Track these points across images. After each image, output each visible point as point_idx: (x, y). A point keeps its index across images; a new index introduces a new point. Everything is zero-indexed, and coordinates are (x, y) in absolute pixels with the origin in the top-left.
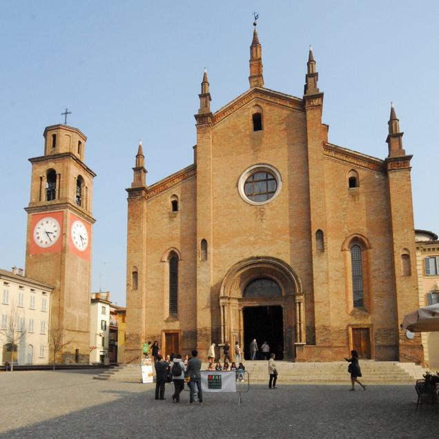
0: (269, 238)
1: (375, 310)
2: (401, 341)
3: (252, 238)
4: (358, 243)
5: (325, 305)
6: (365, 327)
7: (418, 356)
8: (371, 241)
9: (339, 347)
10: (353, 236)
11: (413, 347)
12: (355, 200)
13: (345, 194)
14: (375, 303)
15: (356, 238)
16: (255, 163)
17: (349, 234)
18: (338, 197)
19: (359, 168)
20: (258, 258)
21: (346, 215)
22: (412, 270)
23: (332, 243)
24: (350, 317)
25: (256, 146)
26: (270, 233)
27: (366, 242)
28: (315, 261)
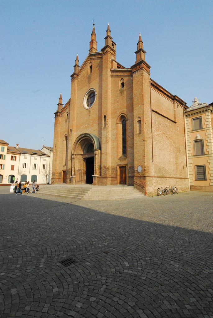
0: (92, 124)
1: (129, 155)
2: (135, 174)
3: (86, 125)
4: (123, 119)
5: (105, 155)
6: (124, 166)
7: (142, 183)
8: (128, 116)
9: (113, 177)
10: (121, 115)
11: (140, 177)
12: (122, 95)
13: (118, 93)
14: (129, 151)
15: (122, 115)
16: (89, 89)
17: (119, 115)
18: (115, 95)
19: (124, 77)
20: (83, 134)
21: (118, 104)
22: (142, 129)
23: (110, 121)
24: (118, 160)
25: (89, 82)
26: (92, 121)
27: (126, 117)
28: (102, 131)
